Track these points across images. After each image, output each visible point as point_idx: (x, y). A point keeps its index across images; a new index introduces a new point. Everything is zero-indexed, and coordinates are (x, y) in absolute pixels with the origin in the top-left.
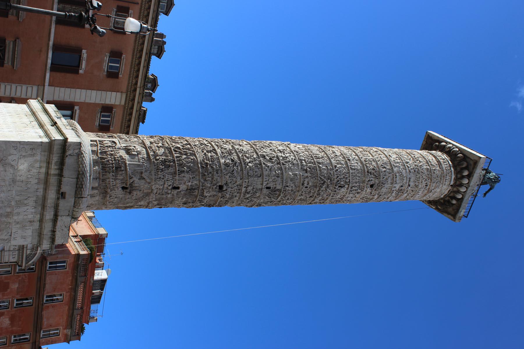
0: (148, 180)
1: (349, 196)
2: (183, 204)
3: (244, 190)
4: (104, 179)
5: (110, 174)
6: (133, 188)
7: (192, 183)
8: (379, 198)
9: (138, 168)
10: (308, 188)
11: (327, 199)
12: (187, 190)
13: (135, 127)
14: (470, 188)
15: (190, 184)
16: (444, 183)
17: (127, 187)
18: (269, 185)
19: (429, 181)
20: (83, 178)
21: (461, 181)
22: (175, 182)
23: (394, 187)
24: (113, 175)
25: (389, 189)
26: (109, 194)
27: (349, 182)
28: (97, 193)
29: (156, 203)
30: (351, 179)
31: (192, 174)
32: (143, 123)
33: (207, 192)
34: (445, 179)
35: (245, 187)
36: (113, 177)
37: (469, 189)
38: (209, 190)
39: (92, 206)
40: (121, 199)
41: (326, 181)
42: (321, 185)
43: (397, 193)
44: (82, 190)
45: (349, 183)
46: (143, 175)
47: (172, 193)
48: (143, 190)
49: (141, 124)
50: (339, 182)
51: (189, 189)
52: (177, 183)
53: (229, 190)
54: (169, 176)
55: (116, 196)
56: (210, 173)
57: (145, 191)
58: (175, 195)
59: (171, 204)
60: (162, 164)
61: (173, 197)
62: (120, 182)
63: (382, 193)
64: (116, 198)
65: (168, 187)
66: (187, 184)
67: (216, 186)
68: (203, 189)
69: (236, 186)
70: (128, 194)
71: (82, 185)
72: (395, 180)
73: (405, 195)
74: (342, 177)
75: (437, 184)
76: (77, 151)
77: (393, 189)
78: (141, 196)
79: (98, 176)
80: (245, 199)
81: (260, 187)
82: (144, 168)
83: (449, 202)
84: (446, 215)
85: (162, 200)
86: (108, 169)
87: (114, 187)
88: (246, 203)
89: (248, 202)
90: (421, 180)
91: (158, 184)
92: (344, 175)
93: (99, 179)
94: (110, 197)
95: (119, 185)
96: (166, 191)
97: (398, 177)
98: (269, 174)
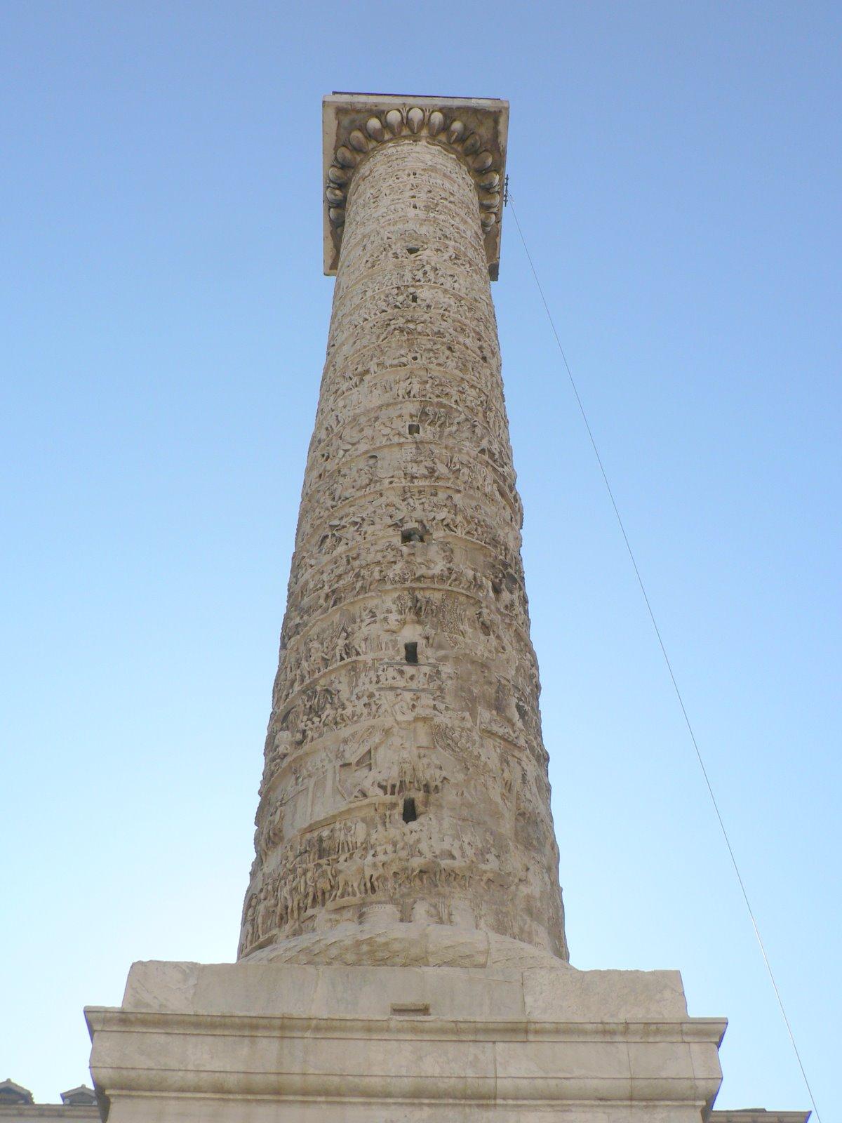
0: (377, 738)
4: (362, 888)
5: (340, 871)
6: (407, 779)
7: (389, 611)
12: (419, 622)
17: (401, 803)
18: (401, 430)
21: (396, 127)
22: (386, 660)
24: (346, 861)
26: (439, 860)
31: (358, 620)
36: (356, 857)
38: (420, 564)
40: (464, 820)
44: (382, 940)
48: (418, 747)
51: (418, 613)
52: (391, 652)
55: (448, 840)
57: (424, 740)
59: (489, 668)
61: (451, 660)
62: (380, 827)
66: (393, 624)
69: (406, 503)
81: (410, 450)
83: (462, 139)
84: (501, 139)
85: (470, 691)
86: (323, 884)
87: (400, 845)
91: (394, 705)
93: (363, 905)
94: (453, 857)
95: (398, 828)
96: (422, 679)
98: (367, 441)
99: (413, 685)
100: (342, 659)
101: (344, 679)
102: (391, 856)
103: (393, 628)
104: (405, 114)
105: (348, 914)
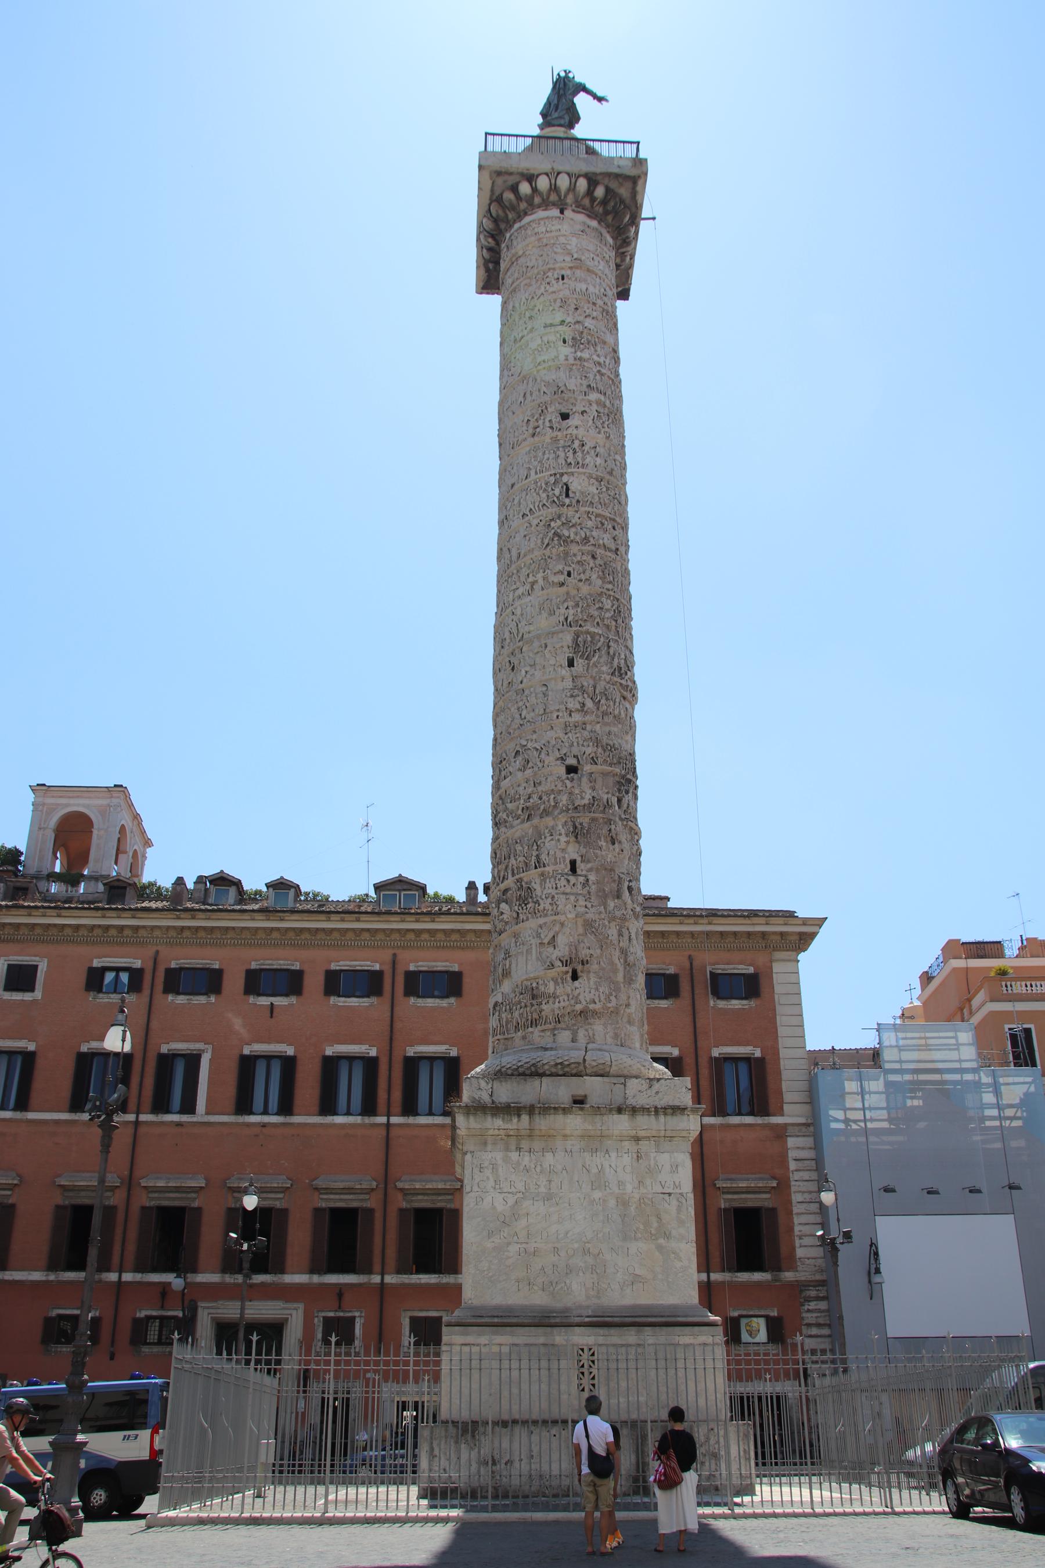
0: (557, 928)
1: (592, 464)
2: (613, 844)
3: (577, 717)
6: (573, 956)
7: (560, 834)
8: (597, 388)
9: (534, 952)
10: (571, 569)
11: (597, 516)
12: (578, 842)
13: (659, 921)
14: (559, 167)
15: (563, 839)
16: (554, 234)
17: (571, 971)
19: (550, 274)
20: (544, 1065)
23: (567, 360)
25: (571, 370)
27: (555, 474)
28: (587, 1030)
29: (611, 904)
30: (550, 473)
32: (668, 899)
33: (582, 798)
34: (547, 235)
35: (570, 715)
36: (550, 1002)
37: (560, 168)
39: (623, 1035)
41: (553, 531)
42: (564, 541)
43: (581, 346)
45: (558, 476)
46: (546, 941)
47: (584, 873)
49: (670, 905)
50: (556, 500)
51: (576, 837)
52: (562, 866)
53: (575, 750)
54: (548, 885)
55: (593, 991)
56: (540, 798)
57: (581, 930)
58: (589, 865)
59: (614, 871)
60: (526, 905)
63: (581, 385)
64: (597, 989)
65: (571, 884)
66: (563, 845)
67: (567, 782)
68: (576, 808)
69: (567, 737)
70: (586, 966)
71: (557, 1064)
72: (550, 363)
73: (589, 322)
74: (544, 495)
75: (559, 250)
76: (483, 1083)
77: (571, 361)
78: (592, 937)
79: (548, 1033)
80: (598, 709)
82: (533, 941)
84: (638, 197)
85: (604, 890)
86: (535, 1016)
87: (571, 997)
88: (612, 703)
89: (607, 699)
90: (550, 298)
92: (541, 491)
93: (554, 1029)
94: (595, 1003)
95: (570, 986)
96: (580, 887)
97: (543, 358)
99: (574, 890)
100: (536, 868)
101: (538, 881)
102: (567, 1003)
103: (563, 847)
104: (553, 182)
105: (548, 1033)
